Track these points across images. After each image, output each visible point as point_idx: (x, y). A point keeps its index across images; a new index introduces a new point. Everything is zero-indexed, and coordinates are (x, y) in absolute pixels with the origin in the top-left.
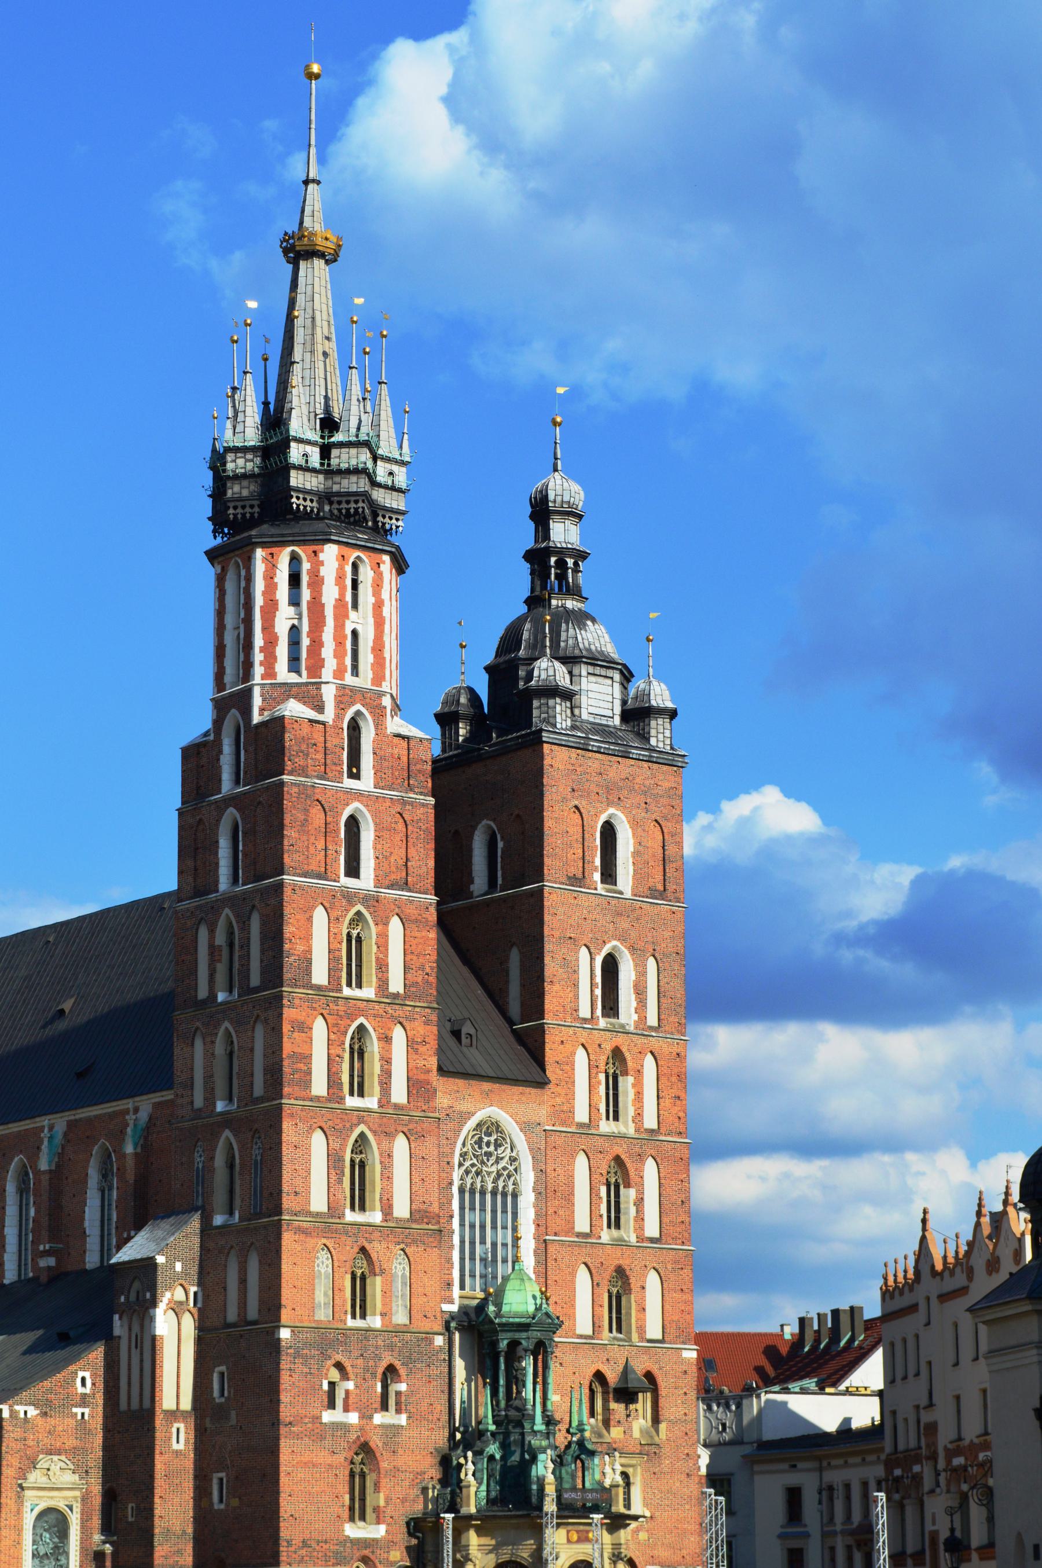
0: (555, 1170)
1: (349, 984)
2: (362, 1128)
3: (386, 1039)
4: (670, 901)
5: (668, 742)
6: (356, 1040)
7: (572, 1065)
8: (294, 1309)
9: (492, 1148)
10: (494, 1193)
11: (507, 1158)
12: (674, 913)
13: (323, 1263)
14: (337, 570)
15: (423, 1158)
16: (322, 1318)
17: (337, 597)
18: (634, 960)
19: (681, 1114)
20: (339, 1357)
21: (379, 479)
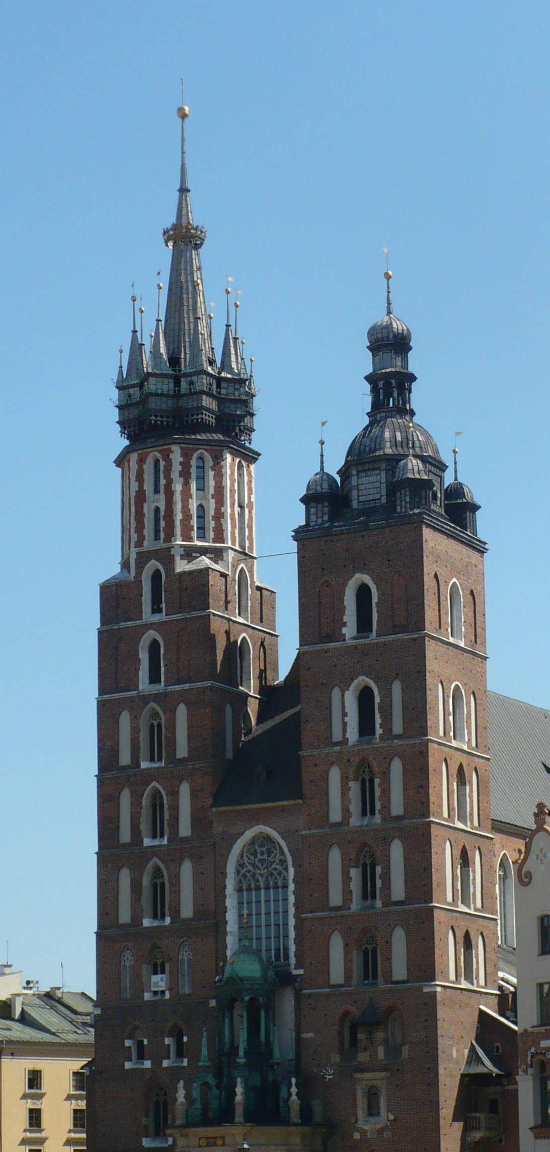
0: (310, 863)
1: (152, 760)
2: (155, 859)
3: (174, 794)
4: (412, 631)
5: (408, 506)
6: (158, 798)
7: (326, 780)
8: (105, 994)
9: (265, 857)
10: (267, 888)
11: (277, 861)
12: (415, 640)
13: (128, 958)
14: (137, 471)
15: (202, 873)
16: (128, 997)
17: (137, 489)
18: (378, 687)
19: (424, 800)
20: (136, 1023)
21: (182, 393)
